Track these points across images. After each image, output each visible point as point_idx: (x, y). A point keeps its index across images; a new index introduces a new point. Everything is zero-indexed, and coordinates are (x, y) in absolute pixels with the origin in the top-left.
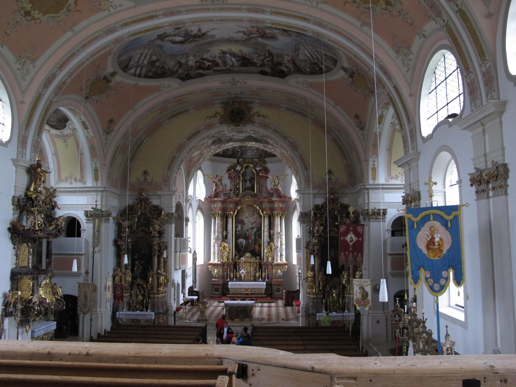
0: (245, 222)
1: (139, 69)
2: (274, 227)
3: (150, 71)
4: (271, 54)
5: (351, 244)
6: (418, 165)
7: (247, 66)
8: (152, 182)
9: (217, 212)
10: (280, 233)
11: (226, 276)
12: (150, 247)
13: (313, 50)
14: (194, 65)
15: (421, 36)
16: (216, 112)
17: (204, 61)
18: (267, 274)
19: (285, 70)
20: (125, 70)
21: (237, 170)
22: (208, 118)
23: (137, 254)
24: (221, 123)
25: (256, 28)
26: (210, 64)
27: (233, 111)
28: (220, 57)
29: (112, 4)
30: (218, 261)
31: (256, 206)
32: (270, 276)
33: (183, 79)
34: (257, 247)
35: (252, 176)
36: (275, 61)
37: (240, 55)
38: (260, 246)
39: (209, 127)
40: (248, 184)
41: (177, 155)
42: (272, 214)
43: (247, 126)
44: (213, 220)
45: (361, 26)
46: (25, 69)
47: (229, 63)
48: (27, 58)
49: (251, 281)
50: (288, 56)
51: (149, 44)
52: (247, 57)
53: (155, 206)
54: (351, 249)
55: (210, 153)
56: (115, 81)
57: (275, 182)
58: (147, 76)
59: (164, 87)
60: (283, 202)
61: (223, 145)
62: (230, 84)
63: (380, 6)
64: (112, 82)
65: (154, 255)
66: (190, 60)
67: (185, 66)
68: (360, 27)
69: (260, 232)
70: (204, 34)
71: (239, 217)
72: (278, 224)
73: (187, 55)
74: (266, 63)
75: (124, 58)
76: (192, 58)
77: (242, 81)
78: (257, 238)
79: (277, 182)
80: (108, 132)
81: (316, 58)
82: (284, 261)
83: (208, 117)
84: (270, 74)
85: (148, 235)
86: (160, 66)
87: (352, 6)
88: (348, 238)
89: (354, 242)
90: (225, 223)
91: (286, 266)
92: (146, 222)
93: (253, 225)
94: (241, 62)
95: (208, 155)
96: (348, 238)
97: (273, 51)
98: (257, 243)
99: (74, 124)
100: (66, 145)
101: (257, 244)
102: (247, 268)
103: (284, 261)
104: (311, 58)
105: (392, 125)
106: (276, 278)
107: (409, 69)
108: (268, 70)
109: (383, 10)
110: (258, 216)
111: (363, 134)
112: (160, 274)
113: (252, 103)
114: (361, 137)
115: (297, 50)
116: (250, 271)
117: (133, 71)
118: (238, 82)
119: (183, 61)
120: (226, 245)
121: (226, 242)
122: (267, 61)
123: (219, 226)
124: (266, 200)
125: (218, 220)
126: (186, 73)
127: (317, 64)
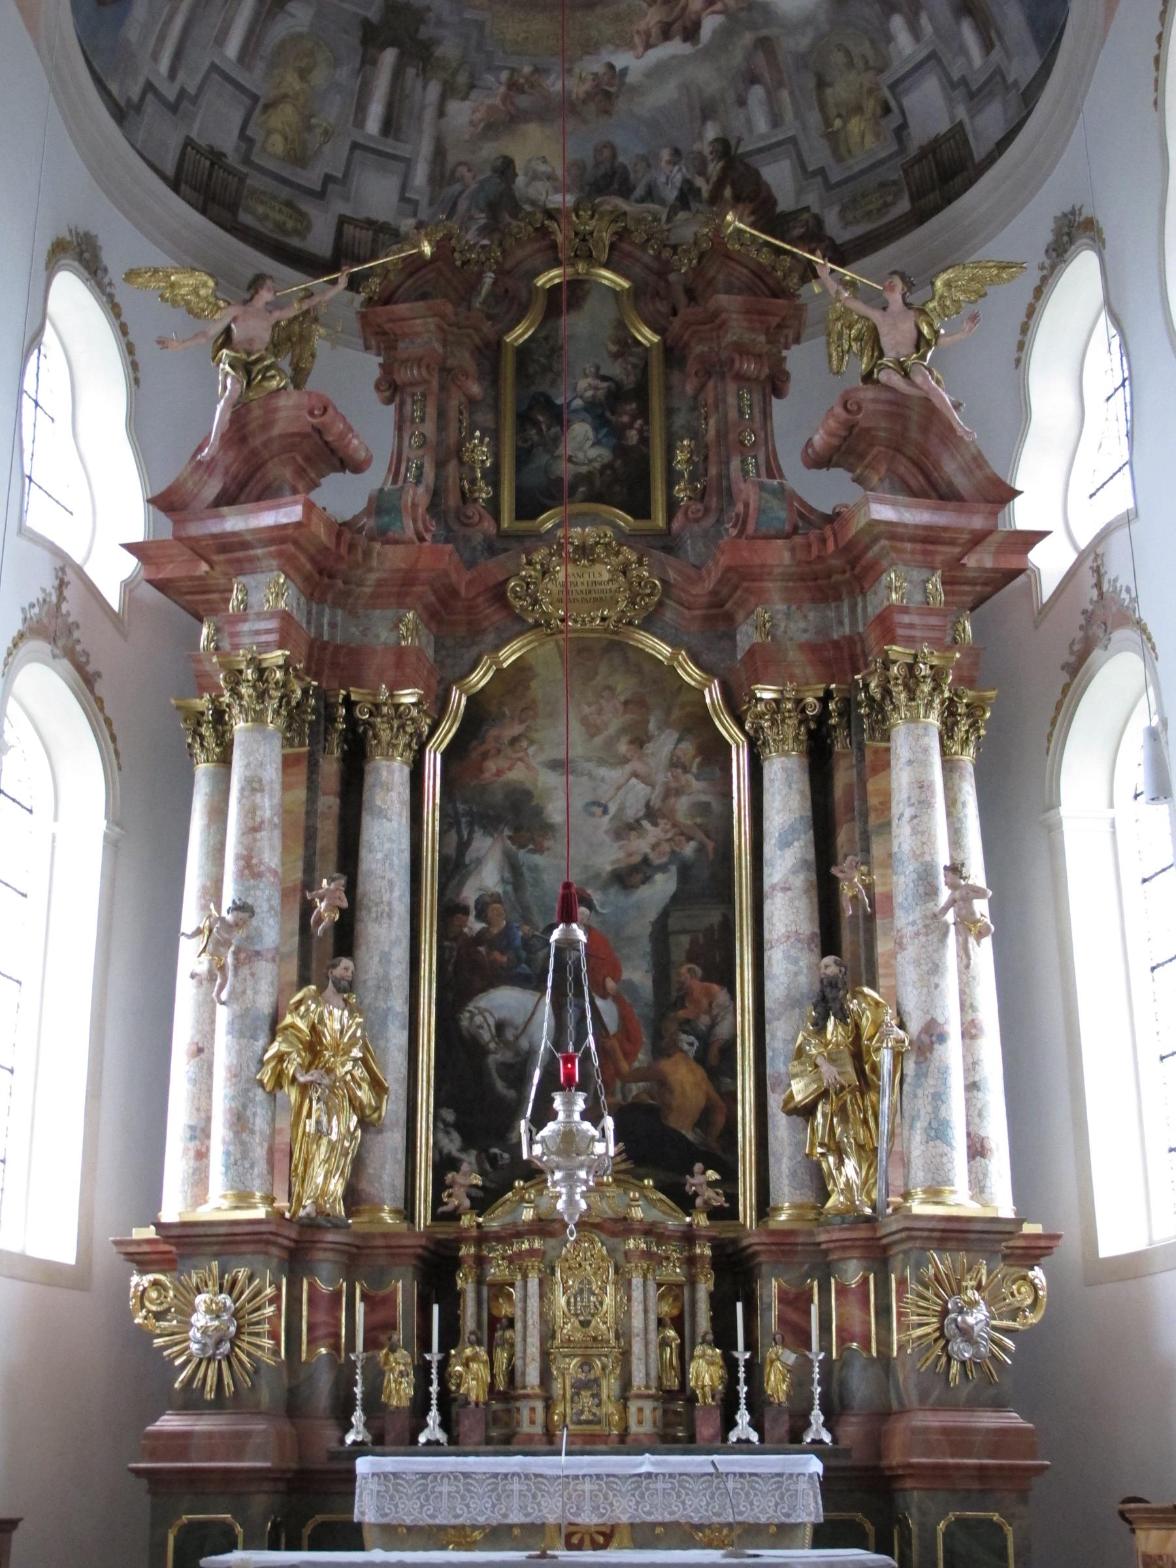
0: (555, 812)
9: (241, 658)
11: (324, 1382)
18: (816, 1355)
30: (243, 1199)
31: (663, 650)
32: (860, 1385)
35: (616, 370)
42: (848, 708)
44: (203, 770)
49: (625, 1444)
71: (491, 766)
72: (923, 786)
78: (687, 974)
82: (1004, 1207)
90: (329, 803)
91: (1038, 1274)
93: (641, 845)
98: (687, 1026)
101: (688, 1042)
106: (946, 1404)
110: (688, 748)
116: (623, 1333)
123: (268, 806)
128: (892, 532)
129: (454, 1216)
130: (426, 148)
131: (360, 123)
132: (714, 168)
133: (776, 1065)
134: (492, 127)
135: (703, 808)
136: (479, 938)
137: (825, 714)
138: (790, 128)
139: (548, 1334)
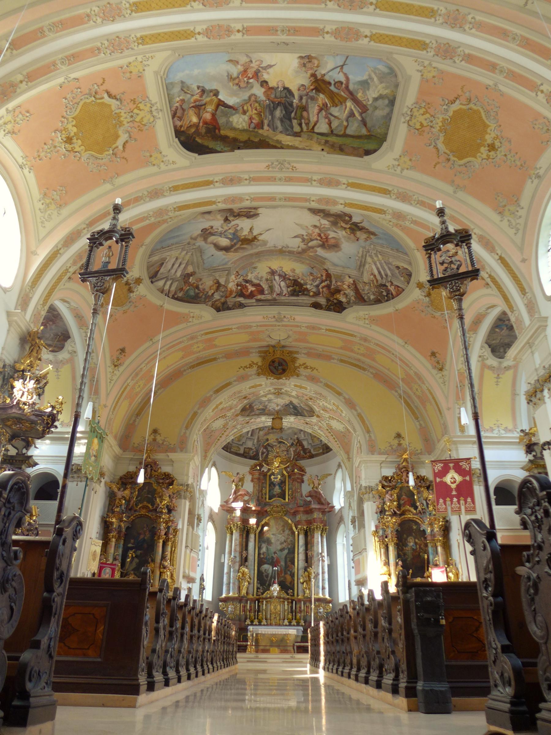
0: (273, 541)
1: (169, 283)
2: (313, 545)
3: (181, 289)
4: (329, 276)
5: (453, 486)
6: (546, 336)
7: (298, 295)
8: (163, 443)
10: (321, 554)
12: (154, 533)
13: (383, 261)
14: (235, 289)
16: (253, 362)
17: (247, 284)
19: (344, 300)
20: (153, 280)
21: (263, 471)
22: (242, 369)
23: (132, 541)
24: (259, 374)
25: (320, 229)
26: (254, 289)
27: (273, 362)
28: (267, 280)
29: (164, 159)
30: (234, 593)
31: (287, 519)
33: (218, 310)
34: (288, 578)
36: (333, 287)
37: (291, 278)
38: (292, 575)
39: (243, 378)
40: (277, 490)
41: (199, 411)
42: (310, 529)
43: (292, 379)
45: (455, 192)
46: (47, 214)
47: (277, 289)
48: (53, 199)
50: (349, 277)
51: (189, 244)
52: (299, 280)
53: (165, 473)
54: (454, 493)
55: (236, 430)
56: (138, 293)
57: (313, 483)
58: (176, 296)
59: (193, 317)
60: (324, 512)
61: (252, 420)
62: (273, 320)
63: (480, 157)
64: (135, 294)
65: (159, 539)
66: (231, 280)
67: (223, 290)
68: (452, 193)
69: (292, 556)
70: (255, 238)
72: (318, 542)
73: (229, 271)
74: (321, 290)
75: (155, 258)
76: (233, 277)
77: (289, 317)
79: (316, 482)
80: (116, 363)
81: (384, 276)
83: (241, 367)
84: (324, 307)
85: (151, 513)
86: (194, 283)
87: (444, 167)
88: (448, 479)
89: (457, 482)
90: (244, 540)
91: (331, 605)
92: (150, 496)
93: (284, 546)
94: (292, 288)
95: (233, 432)
96: (448, 479)
97: (332, 270)
98: (289, 570)
99: (75, 344)
100: (58, 375)
101: (289, 573)
102: (275, 606)
103: (327, 597)
104: (379, 277)
105: (480, 359)
107: (518, 230)
108: (322, 301)
109: (484, 161)
110: (290, 532)
111: (443, 376)
112: (165, 568)
113: (297, 352)
114: (441, 381)
115: (362, 265)
117: (161, 283)
118: (285, 317)
119: (222, 281)
120: (246, 570)
121: (247, 567)
122: (322, 288)
124: (302, 509)
125: (236, 535)
126: (223, 300)
127: (385, 285)
128: (315, 509)
129: (259, 595)
130: (256, 437)
131: (248, 435)
132: (296, 441)
133: (300, 577)
134: (266, 434)
135: (292, 541)
136: (263, 558)
137: (307, 530)
138: (307, 437)
139: (271, 611)
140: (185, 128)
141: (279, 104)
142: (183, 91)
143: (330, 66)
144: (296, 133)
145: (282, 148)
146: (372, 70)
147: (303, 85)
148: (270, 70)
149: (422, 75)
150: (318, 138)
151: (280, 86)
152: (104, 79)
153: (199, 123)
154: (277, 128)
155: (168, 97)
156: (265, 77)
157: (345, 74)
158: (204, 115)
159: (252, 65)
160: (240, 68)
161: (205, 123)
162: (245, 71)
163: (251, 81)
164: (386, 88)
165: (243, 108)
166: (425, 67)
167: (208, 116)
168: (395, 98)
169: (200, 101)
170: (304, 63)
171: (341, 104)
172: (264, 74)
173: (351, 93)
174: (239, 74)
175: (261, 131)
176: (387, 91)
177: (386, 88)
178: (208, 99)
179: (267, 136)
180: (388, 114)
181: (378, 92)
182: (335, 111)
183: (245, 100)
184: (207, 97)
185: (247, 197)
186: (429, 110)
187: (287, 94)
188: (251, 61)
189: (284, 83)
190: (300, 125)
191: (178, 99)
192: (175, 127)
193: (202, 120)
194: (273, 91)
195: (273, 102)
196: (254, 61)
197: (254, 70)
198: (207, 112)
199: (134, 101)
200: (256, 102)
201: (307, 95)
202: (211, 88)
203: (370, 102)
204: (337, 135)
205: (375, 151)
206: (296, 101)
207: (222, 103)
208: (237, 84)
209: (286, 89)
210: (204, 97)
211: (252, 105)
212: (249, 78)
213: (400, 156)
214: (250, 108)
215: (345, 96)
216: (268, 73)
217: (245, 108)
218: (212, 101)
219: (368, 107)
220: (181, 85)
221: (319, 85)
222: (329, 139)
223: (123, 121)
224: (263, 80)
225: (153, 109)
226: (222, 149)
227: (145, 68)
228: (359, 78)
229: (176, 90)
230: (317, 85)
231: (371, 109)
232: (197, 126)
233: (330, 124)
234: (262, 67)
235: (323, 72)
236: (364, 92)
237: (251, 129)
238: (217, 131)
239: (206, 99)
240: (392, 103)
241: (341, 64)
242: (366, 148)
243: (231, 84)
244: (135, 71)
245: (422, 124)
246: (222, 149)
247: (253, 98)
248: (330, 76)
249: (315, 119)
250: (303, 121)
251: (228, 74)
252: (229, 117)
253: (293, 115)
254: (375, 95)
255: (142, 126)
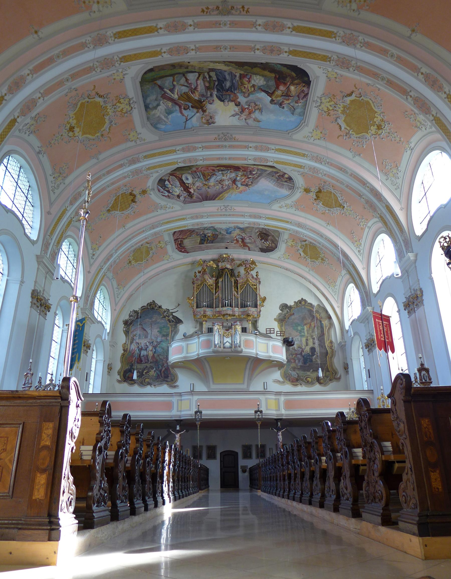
15: (40, 149)
48: (415, 120)
140: (301, 84)
141: (227, 91)
142: (294, 108)
143: (194, 119)
144: (213, 71)
145: (224, 62)
146: (167, 123)
147: (211, 104)
148: (233, 113)
149: (136, 132)
150: (195, 69)
151: (226, 101)
152: (338, 138)
153: (289, 85)
154: (229, 74)
155: (305, 108)
156: (237, 109)
157: (183, 115)
158: (284, 89)
159: (245, 117)
160: (253, 116)
161: (285, 84)
162: (250, 113)
163: (247, 107)
164: (154, 115)
165: (254, 89)
166: (138, 138)
167: (282, 88)
168: (146, 110)
169: (285, 99)
170: (211, 119)
171: (181, 95)
172: (238, 111)
173: (176, 104)
174: (254, 112)
175: (242, 72)
176: (153, 113)
177: (154, 115)
178: (279, 99)
179: (237, 69)
180: (146, 99)
181: (158, 110)
182: (185, 89)
183: (252, 94)
184: (279, 100)
185: (259, 28)
186: (120, 113)
187: (221, 97)
188: (245, 119)
189: (224, 104)
190: (210, 77)
191: (300, 104)
192: (309, 87)
193: (287, 86)
194: (232, 99)
195: (232, 91)
196: (244, 119)
197: (244, 114)
198: (282, 91)
199: (329, 114)
200: (244, 92)
201: (207, 98)
202: (275, 105)
203: (161, 102)
204: (179, 73)
205: (145, 73)
206: (215, 93)
207: (269, 94)
208: (256, 105)
209: (222, 101)
210: (281, 101)
211: (247, 90)
212: (248, 108)
213: (124, 78)
214: (249, 88)
215: (180, 101)
216: (235, 111)
217: (253, 89)
218: (276, 97)
219: (162, 99)
220: (295, 113)
221: (199, 105)
222: (185, 70)
223: (343, 107)
224: (239, 107)
225: (319, 104)
226: (276, 65)
227: (312, 131)
228: (174, 114)
229: (298, 111)
230: (201, 105)
231: (159, 97)
232: (292, 83)
233: (187, 80)
234: (239, 115)
235: (198, 114)
236: (167, 107)
237: (250, 74)
238: (277, 77)
239: (280, 99)
240: (147, 107)
241: (187, 122)
242: (153, 72)
243: (261, 106)
244: (319, 132)
245: (120, 103)
246: (276, 65)
247: (246, 95)
248: (193, 112)
249: (199, 82)
250: (208, 79)
251: (261, 113)
252: (266, 84)
253: (216, 83)
254: (159, 108)
255: (332, 98)
